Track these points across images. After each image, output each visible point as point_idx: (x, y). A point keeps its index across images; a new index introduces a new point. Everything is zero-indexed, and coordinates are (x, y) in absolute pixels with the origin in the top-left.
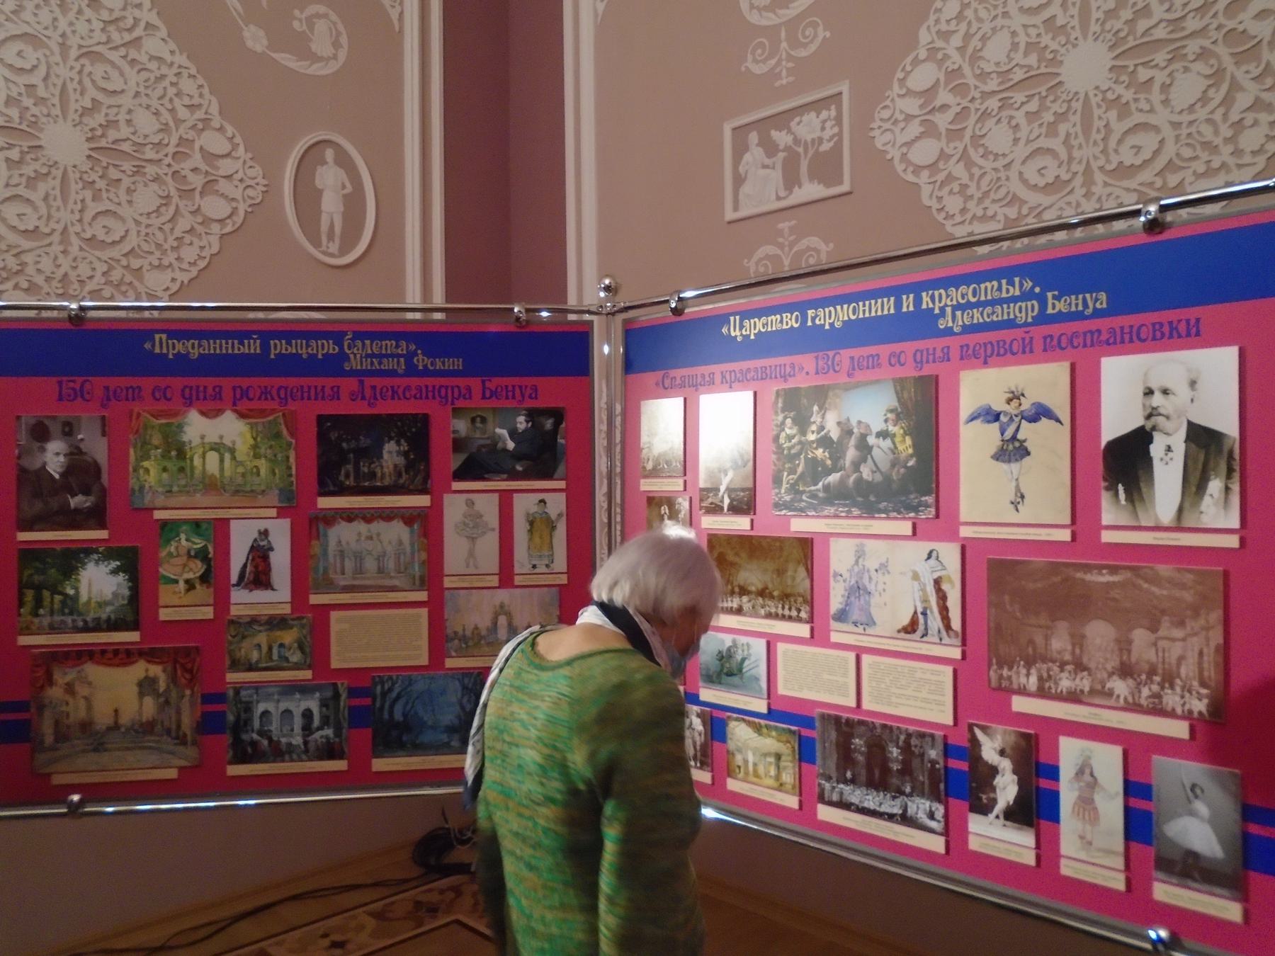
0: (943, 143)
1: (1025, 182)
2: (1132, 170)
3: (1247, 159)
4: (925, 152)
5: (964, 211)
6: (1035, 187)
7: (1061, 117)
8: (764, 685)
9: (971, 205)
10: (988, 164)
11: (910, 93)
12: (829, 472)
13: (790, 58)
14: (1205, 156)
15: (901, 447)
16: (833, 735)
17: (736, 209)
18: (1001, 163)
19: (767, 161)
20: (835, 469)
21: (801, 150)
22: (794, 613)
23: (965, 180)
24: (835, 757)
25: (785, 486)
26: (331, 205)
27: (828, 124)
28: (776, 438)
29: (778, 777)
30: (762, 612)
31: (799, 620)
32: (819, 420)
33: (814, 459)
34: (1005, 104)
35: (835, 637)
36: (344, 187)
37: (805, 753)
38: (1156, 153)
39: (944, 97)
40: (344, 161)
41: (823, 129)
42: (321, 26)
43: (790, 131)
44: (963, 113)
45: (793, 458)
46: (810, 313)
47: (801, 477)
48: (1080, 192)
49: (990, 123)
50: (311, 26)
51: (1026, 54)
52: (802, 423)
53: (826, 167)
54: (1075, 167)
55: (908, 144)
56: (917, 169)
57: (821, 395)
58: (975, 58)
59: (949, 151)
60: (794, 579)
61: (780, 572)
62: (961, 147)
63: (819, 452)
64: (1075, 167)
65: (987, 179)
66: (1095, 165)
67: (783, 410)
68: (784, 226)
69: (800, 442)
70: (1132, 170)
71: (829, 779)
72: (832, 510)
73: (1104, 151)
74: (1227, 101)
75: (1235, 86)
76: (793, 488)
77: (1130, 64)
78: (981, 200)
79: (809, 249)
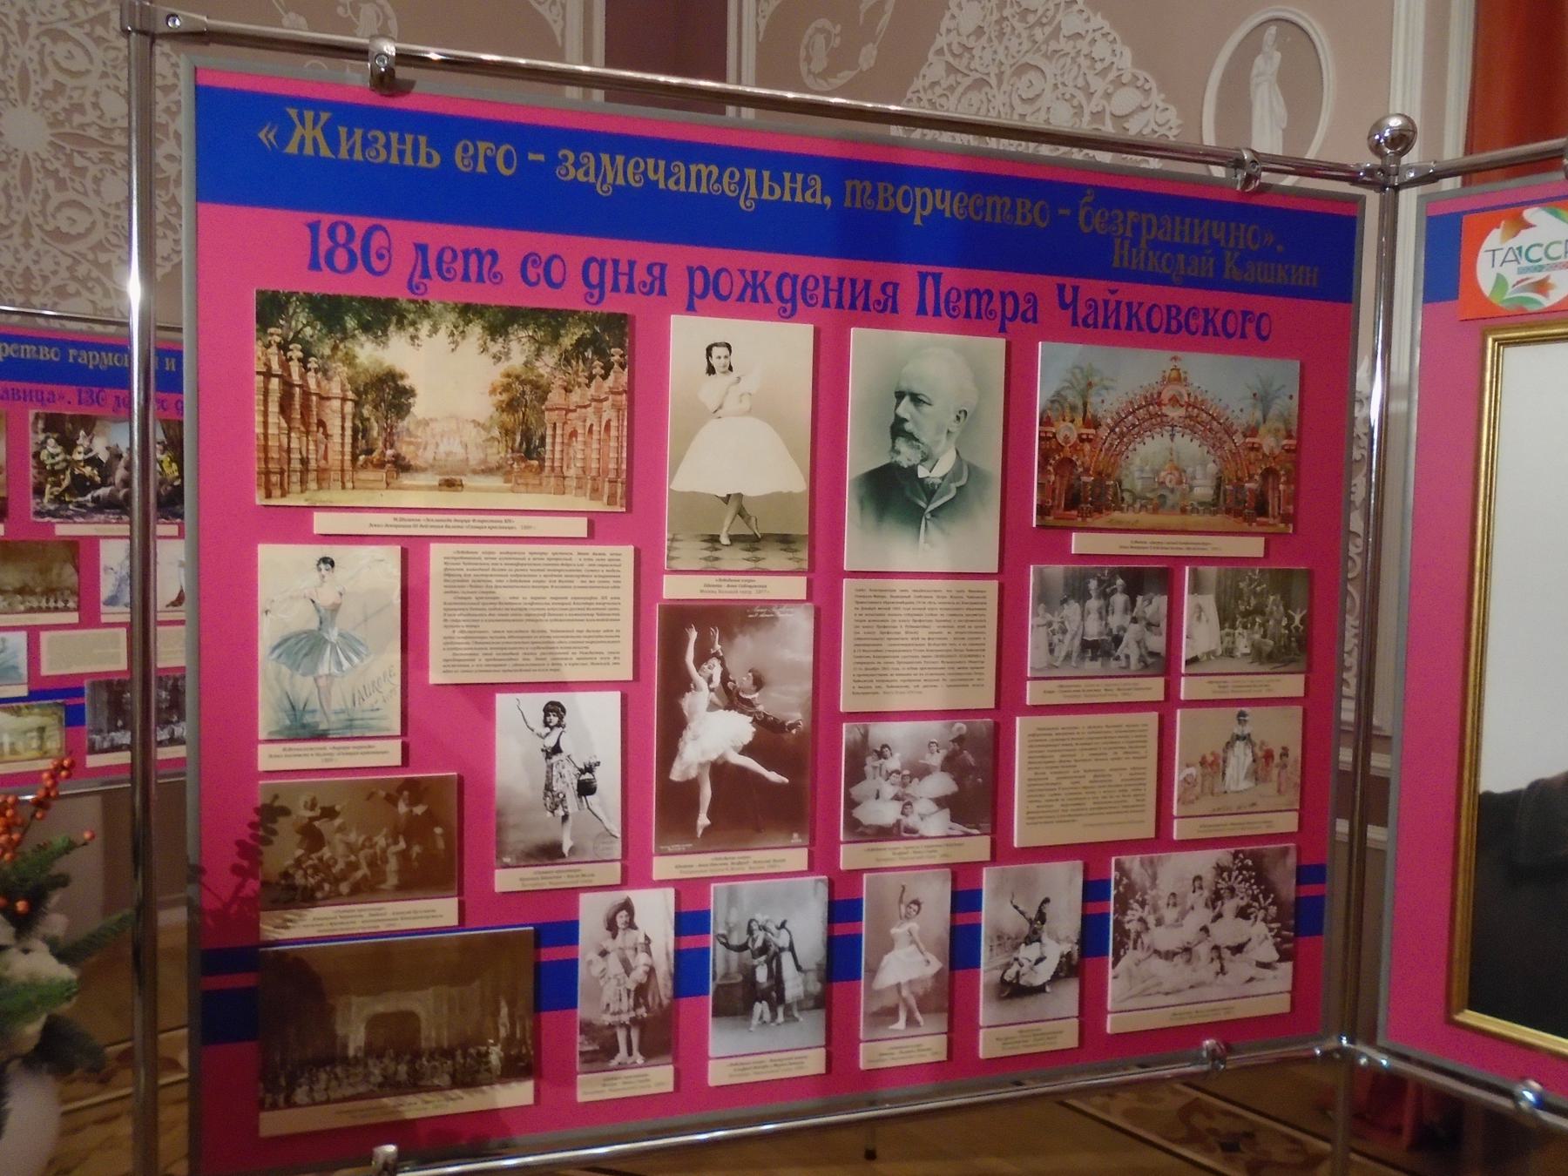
8: (24, 670)
12: (98, 487)
15: (167, 471)
16: (104, 696)
20: (104, 484)
22: (61, 604)
24: (106, 713)
25: (47, 496)
28: (37, 455)
29: (40, 748)
30: (22, 608)
31: (66, 609)
32: (86, 443)
33: (82, 476)
35: (104, 619)
37: (73, 718)
38: (89, 231)
45: (54, 473)
46: (72, 352)
47: (67, 489)
48: (17, 241)
52: (68, 445)
57: (88, 423)
60: (59, 575)
61: (44, 571)
63: (88, 470)
64: (14, 216)
66: (34, 221)
67: (44, 431)
69: (65, 460)
71: (99, 732)
72: (102, 517)
73: (43, 212)
76: (58, 499)
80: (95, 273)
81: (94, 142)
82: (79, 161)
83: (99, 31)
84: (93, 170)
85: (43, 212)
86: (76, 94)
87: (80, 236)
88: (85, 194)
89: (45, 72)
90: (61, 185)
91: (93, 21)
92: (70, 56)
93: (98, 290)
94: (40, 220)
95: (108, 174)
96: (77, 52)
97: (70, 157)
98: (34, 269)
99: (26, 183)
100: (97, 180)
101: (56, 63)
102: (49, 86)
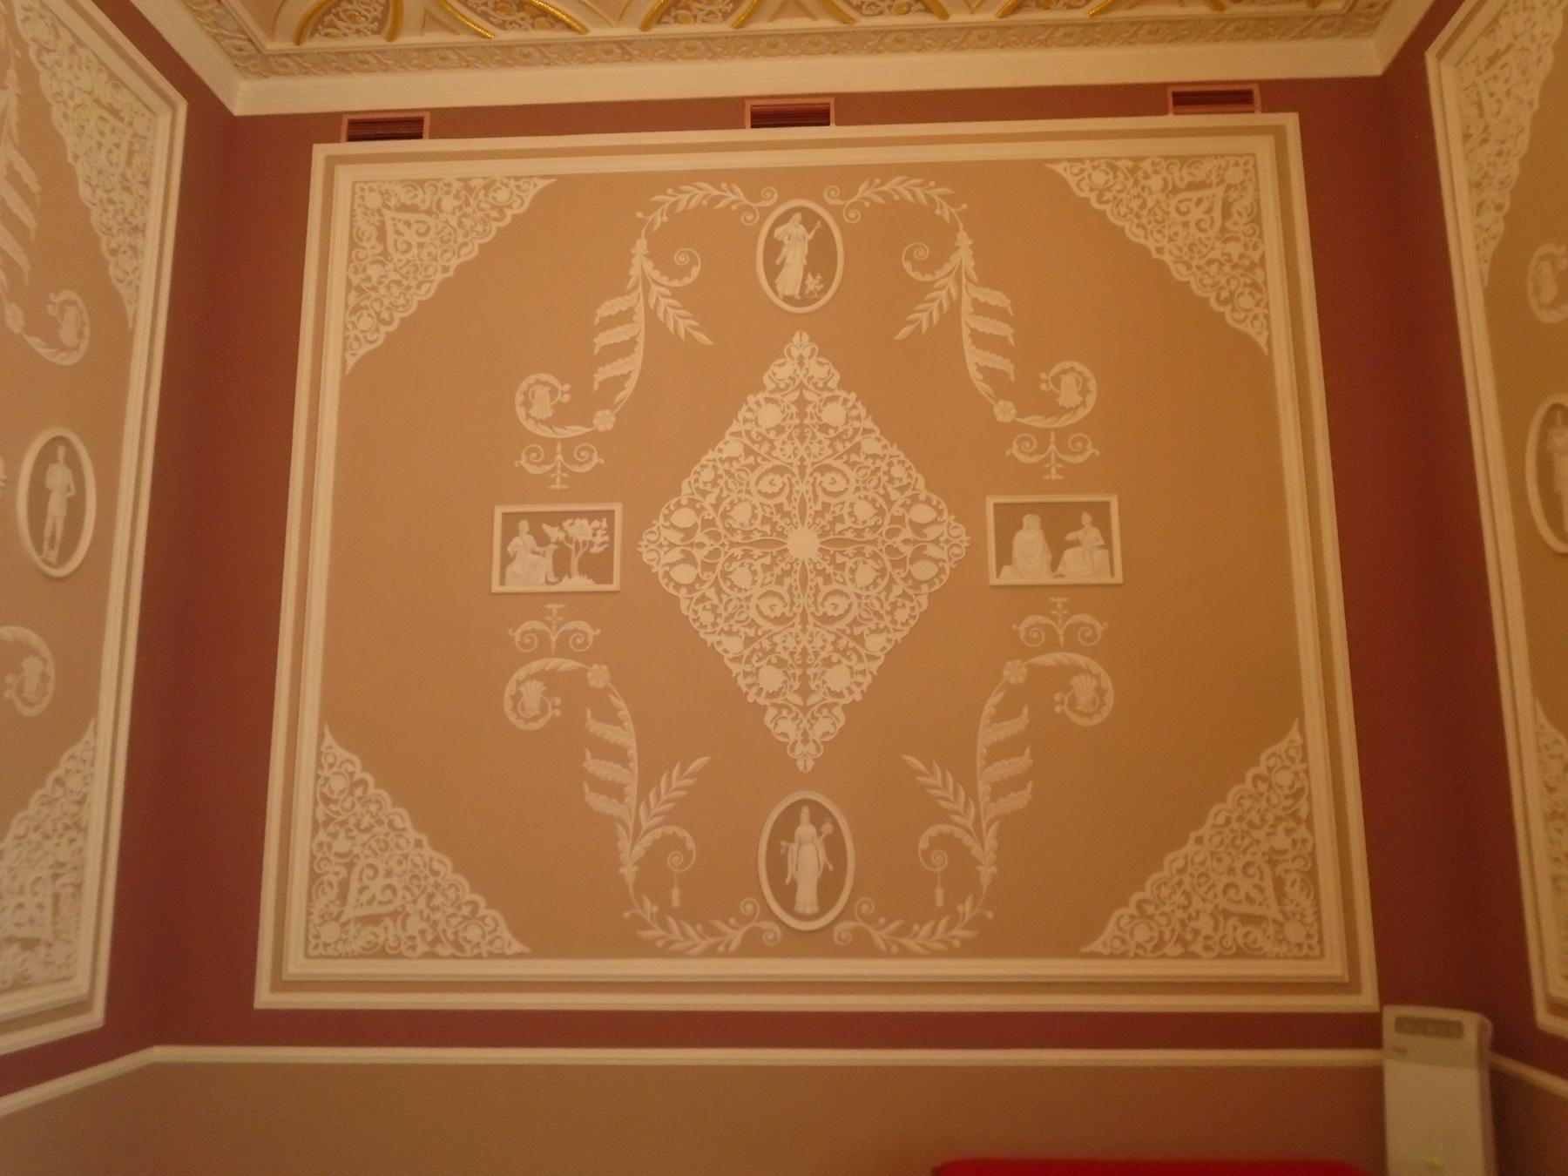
0: (699, 570)
1: (760, 612)
2: (832, 620)
3: (899, 627)
4: (685, 574)
5: (714, 624)
6: (766, 618)
7: (786, 573)
9: (720, 621)
10: (734, 594)
11: (673, 526)
13: (564, 469)
14: (875, 620)
17: (502, 583)
18: (743, 595)
19: (537, 549)
21: (572, 547)
23: (715, 601)
26: (56, 508)
27: (599, 533)
34: (747, 554)
36: (69, 490)
39: (700, 537)
40: (74, 464)
41: (594, 535)
42: (71, 313)
43: (562, 529)
44: (715, 554)
49: (735, 565)
50: (62, 311)
51: (763, 523)
53: (597, 566)
54: (795, 609)
55: (672, 565)
56: (678, 586)
58: (725, 516)
59: (704, 577)
62: (713, 577)
65: (732, 605)
68: (554, 607)
70: (832, 620)
74: (888, 589)
75: (892, 581)
77: (832, 550)
78: (727, 619)
79: (576, 630)
80: (852, 645)
81: (852, 542)
82: (839, 559)
83: (854, 457)
84: (850, 564)
85: (815, 603)
86: (837, 509)
87: (841, 617)
88: (844, 583)
89: (816, 497)
90: (827, 580)
91: (848, 452)
92: (834, 482)
93: (854, 657)
94: (813, 609)
95: (861, 566)
96: (838, 477)
97: (833, 557)
98: (809, 647)
99: (804, 581)
100: (852, 571)
101: (824, 490)
102: (819, 507)
